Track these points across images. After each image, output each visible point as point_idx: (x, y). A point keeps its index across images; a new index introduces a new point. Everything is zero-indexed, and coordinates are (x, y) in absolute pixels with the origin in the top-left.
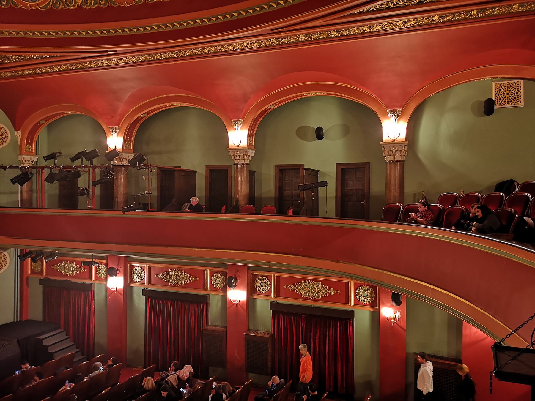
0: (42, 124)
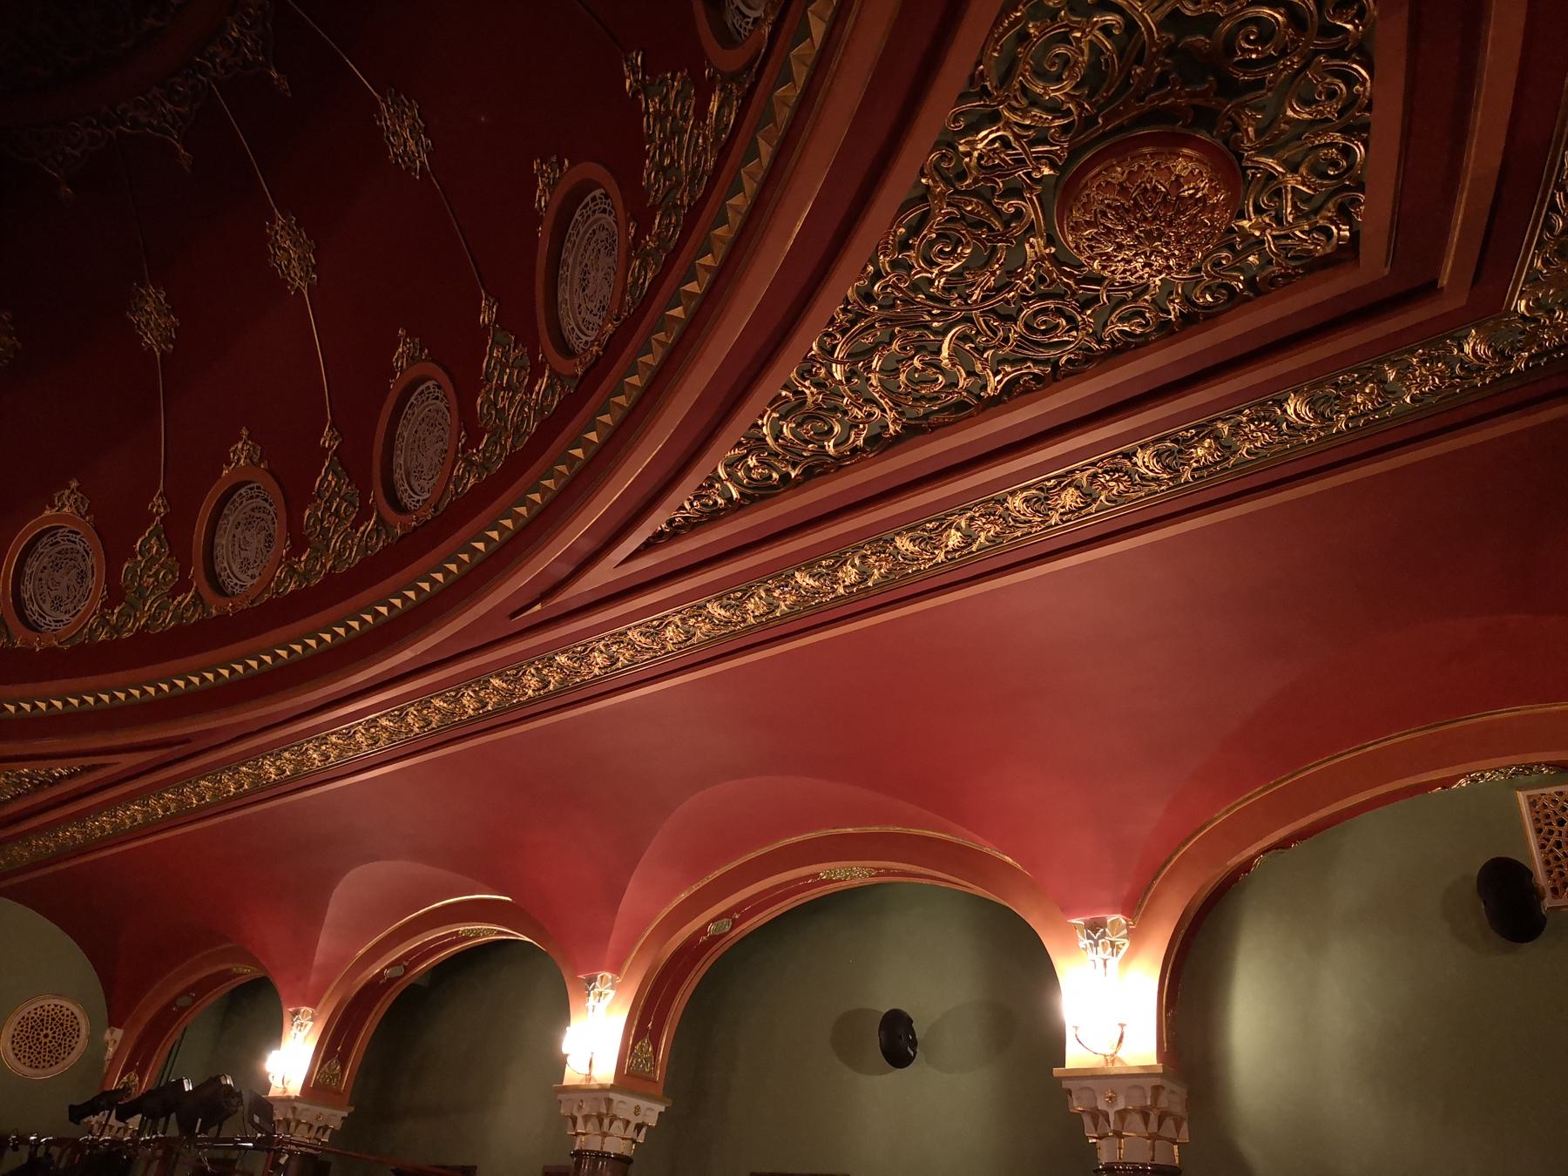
0: (183, 1010)
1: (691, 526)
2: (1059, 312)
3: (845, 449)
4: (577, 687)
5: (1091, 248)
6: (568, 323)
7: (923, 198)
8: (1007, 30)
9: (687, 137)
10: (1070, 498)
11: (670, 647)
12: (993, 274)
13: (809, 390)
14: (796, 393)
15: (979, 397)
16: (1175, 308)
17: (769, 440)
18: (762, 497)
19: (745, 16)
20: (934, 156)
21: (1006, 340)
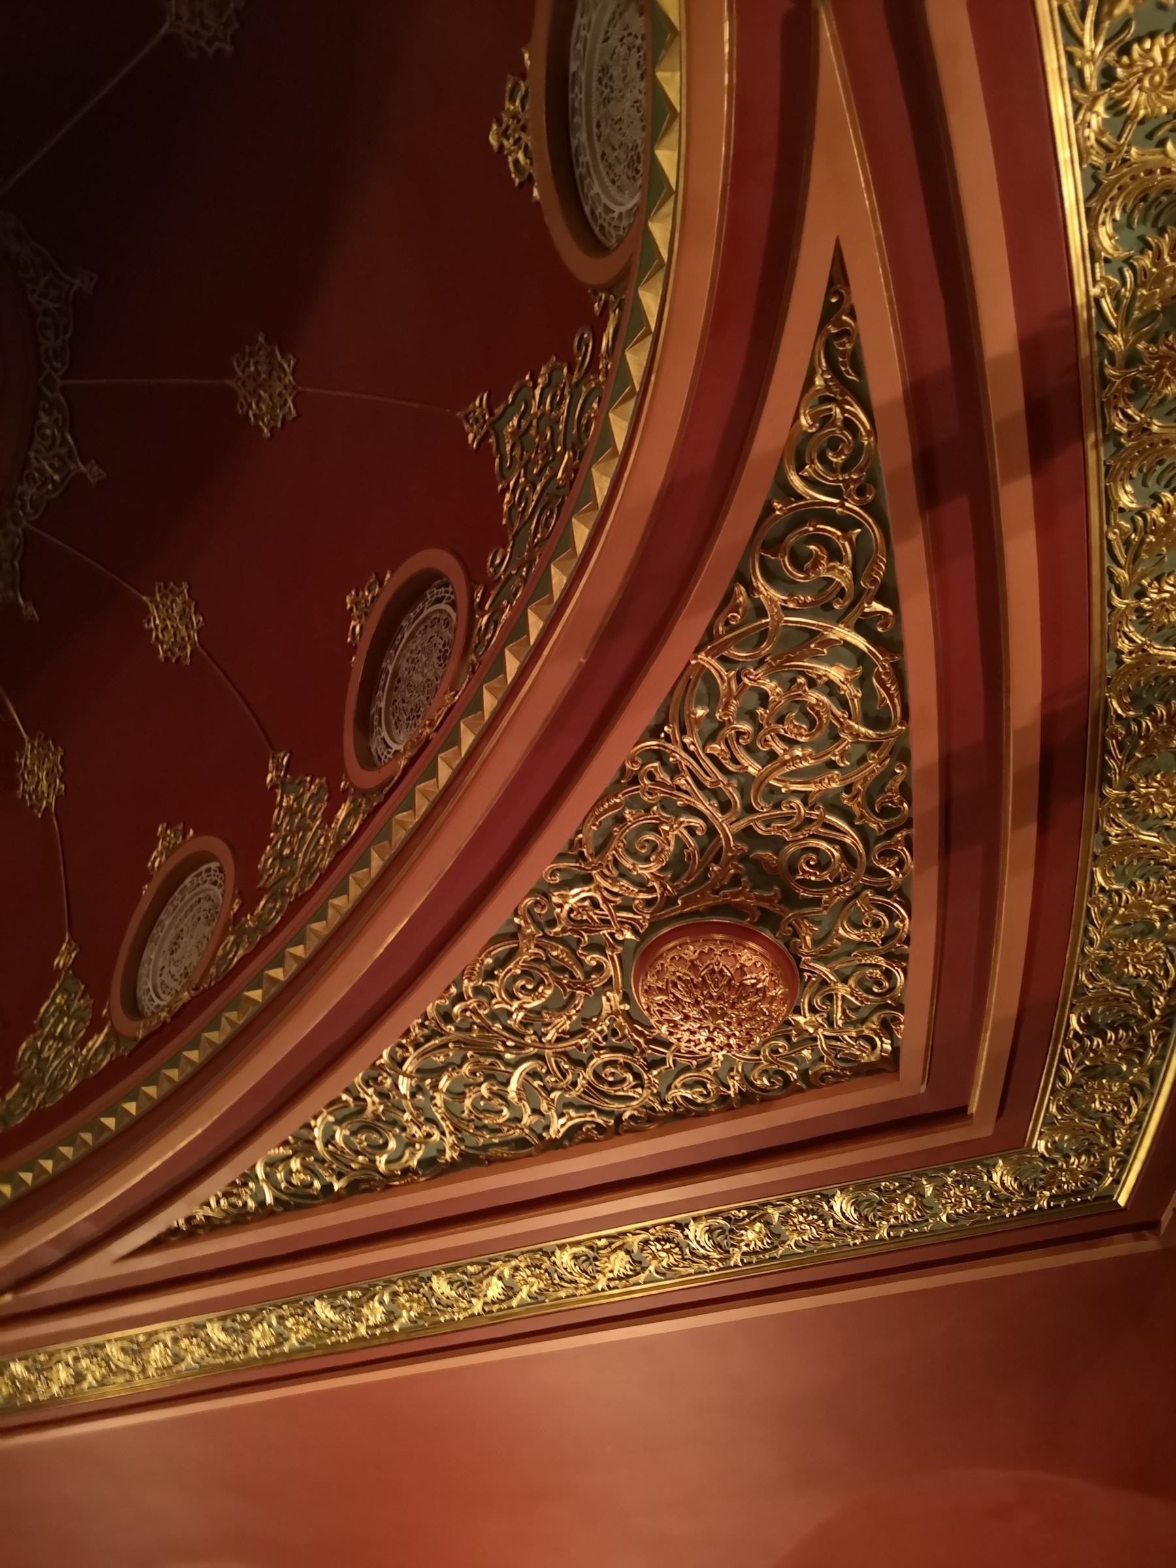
1: (212, 1227)
2: (628, 1067)
3: (397, 1169)
4: (27, 1407)
5: (661, 1013)
6: (146, 983)
7: (514, 936)
8: (606, 811)
9: (310, 834)
10: (619, 1263)
11: (151, 1371)
12: (569, 1018)
13: (370, 1096)
14: (357, 1099)
15: (540, 1137)
16: (734, 1085)
17: (319, 1144)
18: (298, 1207)
19: (388, 747)
20: (529, 901)
21: (574, 1084)
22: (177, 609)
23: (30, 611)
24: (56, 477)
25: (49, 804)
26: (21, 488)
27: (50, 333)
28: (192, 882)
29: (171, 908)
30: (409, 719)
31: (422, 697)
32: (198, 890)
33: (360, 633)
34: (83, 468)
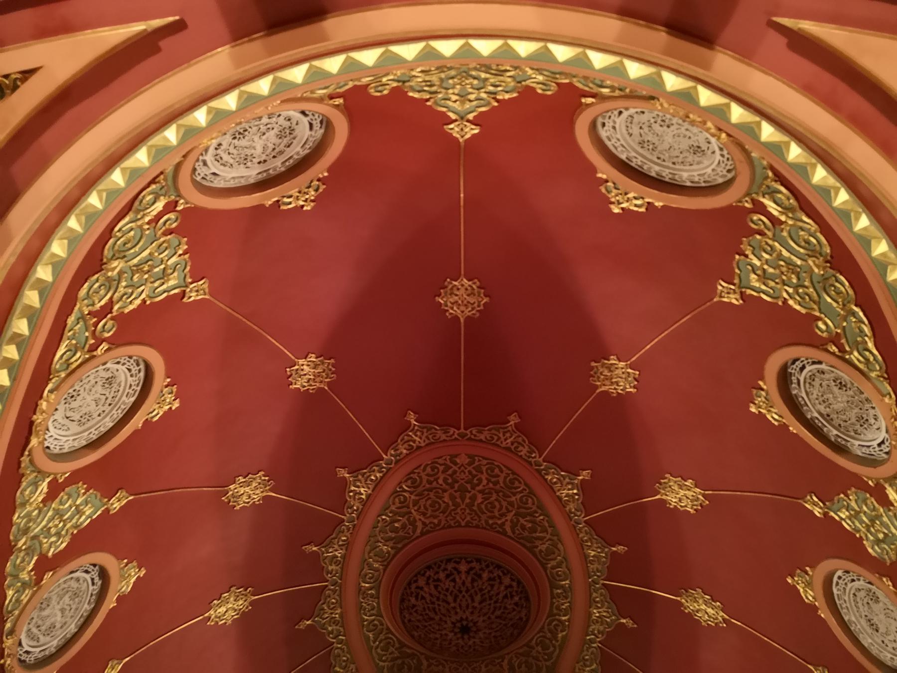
19: (869, 447)
22: (676, 488)
23: (620, 549)
24: (575, 491)
25: (722, 617)
26: (567, 509)
27: (520, 448)
28: (838, 590)
29: (845, 611)
30: (861, 426)
31: (857, 410)
32: (847, 591)
33: (780, 416)
34: (580, 478)
